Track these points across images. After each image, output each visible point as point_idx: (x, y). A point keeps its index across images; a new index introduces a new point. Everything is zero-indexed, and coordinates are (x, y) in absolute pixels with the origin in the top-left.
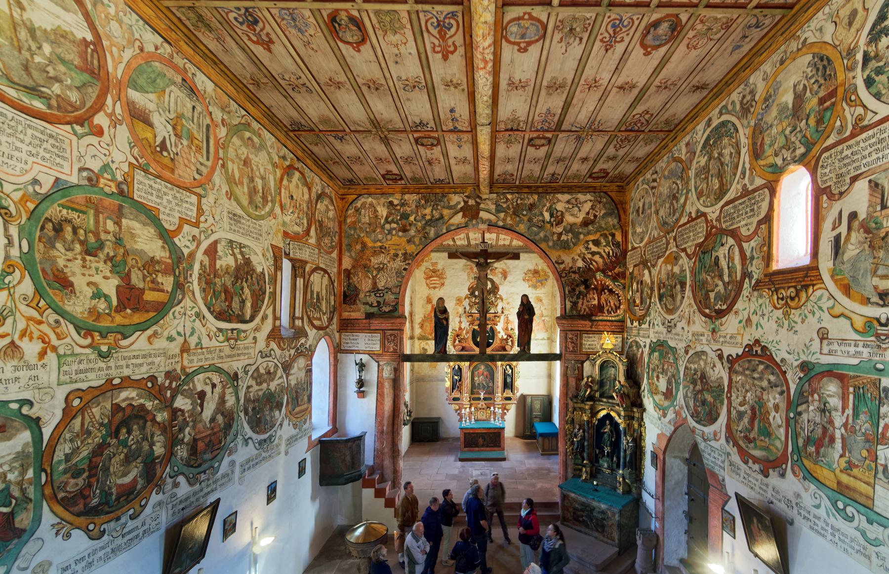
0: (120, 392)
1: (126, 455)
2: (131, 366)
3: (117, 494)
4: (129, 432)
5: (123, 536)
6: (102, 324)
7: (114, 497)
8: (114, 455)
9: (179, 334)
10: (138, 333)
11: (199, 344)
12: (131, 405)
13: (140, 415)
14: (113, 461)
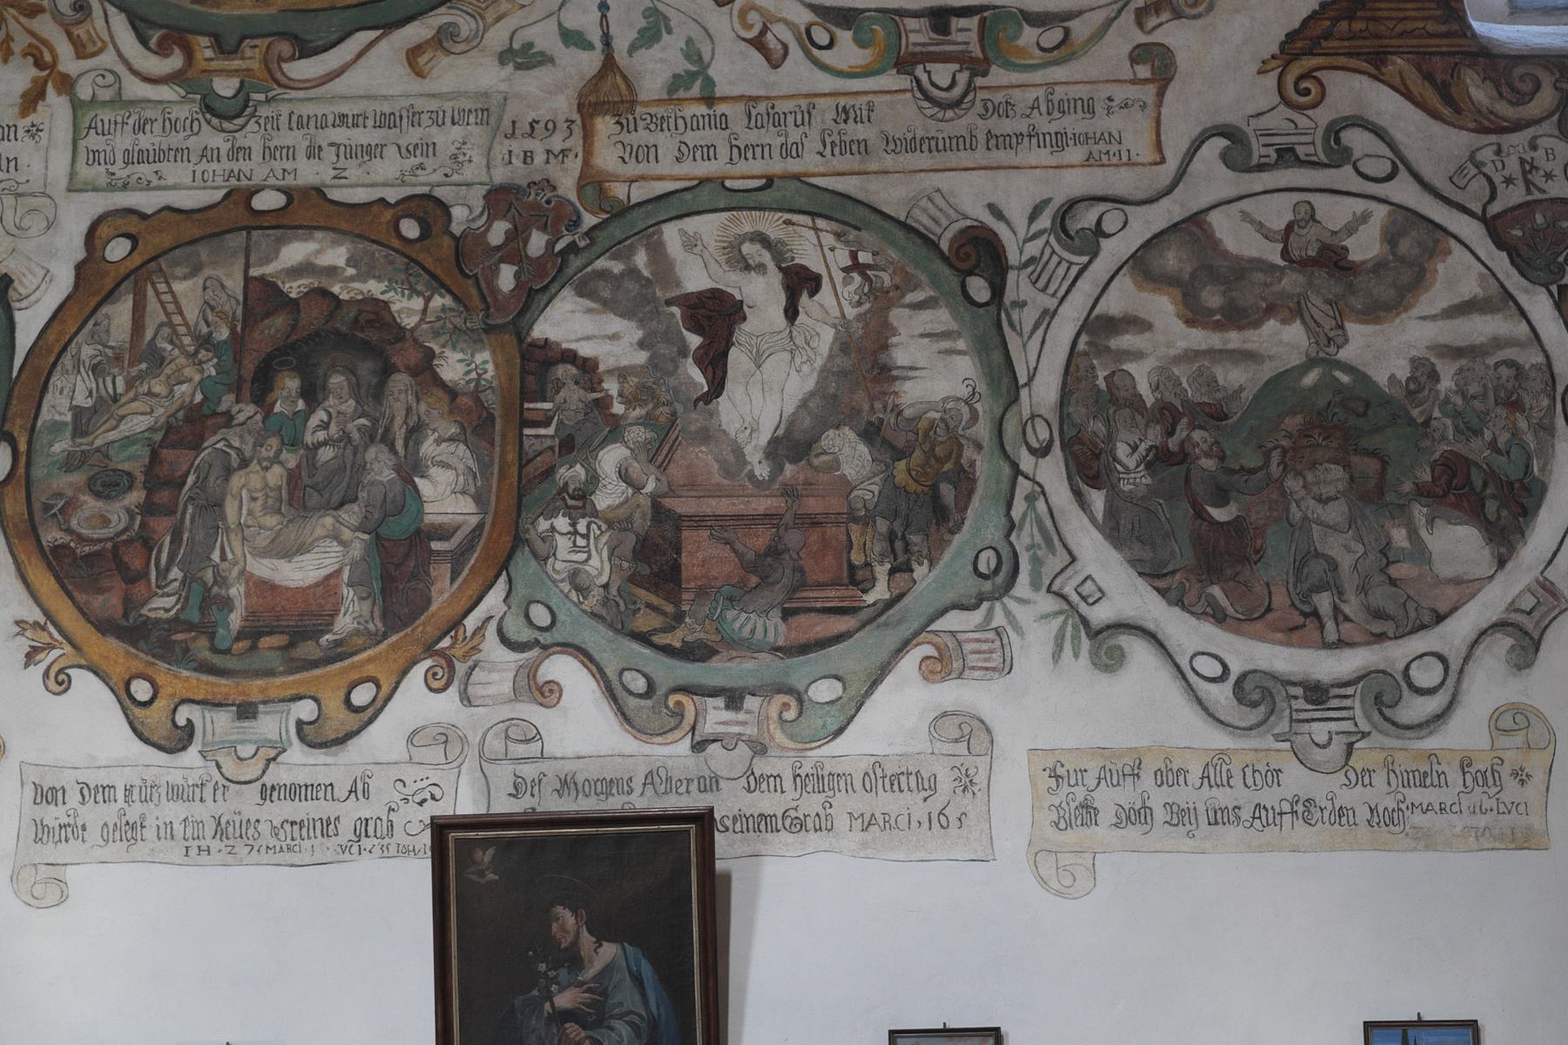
0: (280, 242)
1: (293, 477)
2: (329, 154)
3: (251, 615)
4: (312, 394)
5: (267, 793)
6: (224, 11)
7: (236, 620)
8: (245, 463)
9: (573, 38)
10: (373, 34)
11: (692, 79)
12: (324, 293)
13: (368, 340)
14: (236, 481)
